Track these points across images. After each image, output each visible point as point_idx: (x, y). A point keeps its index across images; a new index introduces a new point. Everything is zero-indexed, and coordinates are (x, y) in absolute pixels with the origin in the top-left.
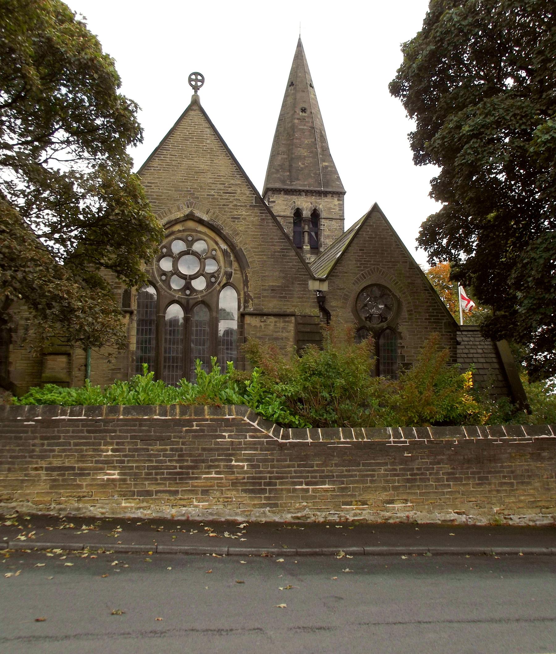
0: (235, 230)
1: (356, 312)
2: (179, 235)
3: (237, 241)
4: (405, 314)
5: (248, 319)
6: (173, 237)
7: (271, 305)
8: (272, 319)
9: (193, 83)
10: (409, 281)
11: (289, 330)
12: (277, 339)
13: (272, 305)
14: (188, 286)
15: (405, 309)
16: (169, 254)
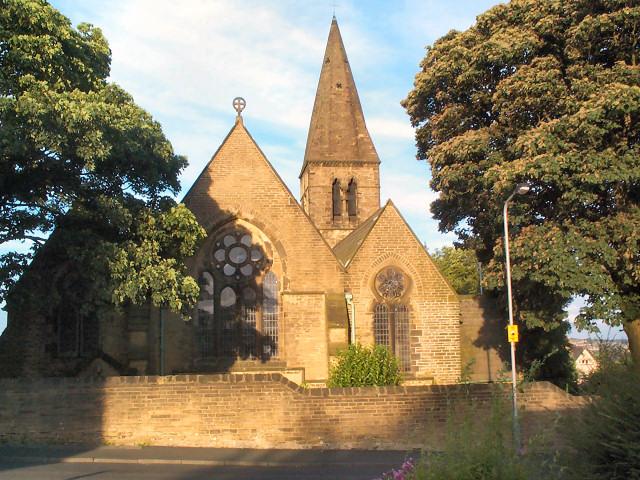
0: (273, 226)
1: (374, 288)
2: (228, 231)
3: (277, 234)
4: (415, 290)
5: (286, 296)
6: (224, 233)
7: (305, 286)
8: (307, 297)
9: (237, 106)
10: (419, 262)
11: (320, 306)
12: (311, 313)
13: (307, 286)
14: (238, 272)
15: (415, 285)
16: (223, 246)
